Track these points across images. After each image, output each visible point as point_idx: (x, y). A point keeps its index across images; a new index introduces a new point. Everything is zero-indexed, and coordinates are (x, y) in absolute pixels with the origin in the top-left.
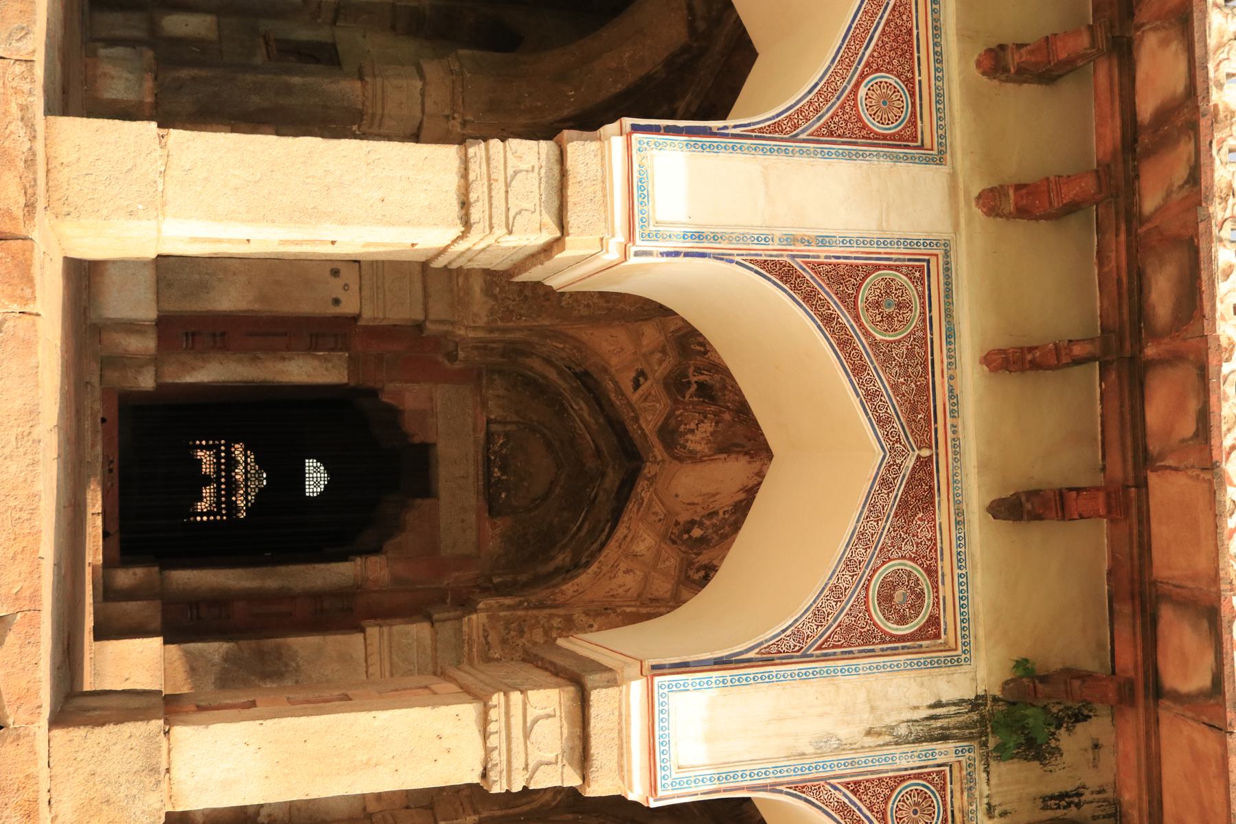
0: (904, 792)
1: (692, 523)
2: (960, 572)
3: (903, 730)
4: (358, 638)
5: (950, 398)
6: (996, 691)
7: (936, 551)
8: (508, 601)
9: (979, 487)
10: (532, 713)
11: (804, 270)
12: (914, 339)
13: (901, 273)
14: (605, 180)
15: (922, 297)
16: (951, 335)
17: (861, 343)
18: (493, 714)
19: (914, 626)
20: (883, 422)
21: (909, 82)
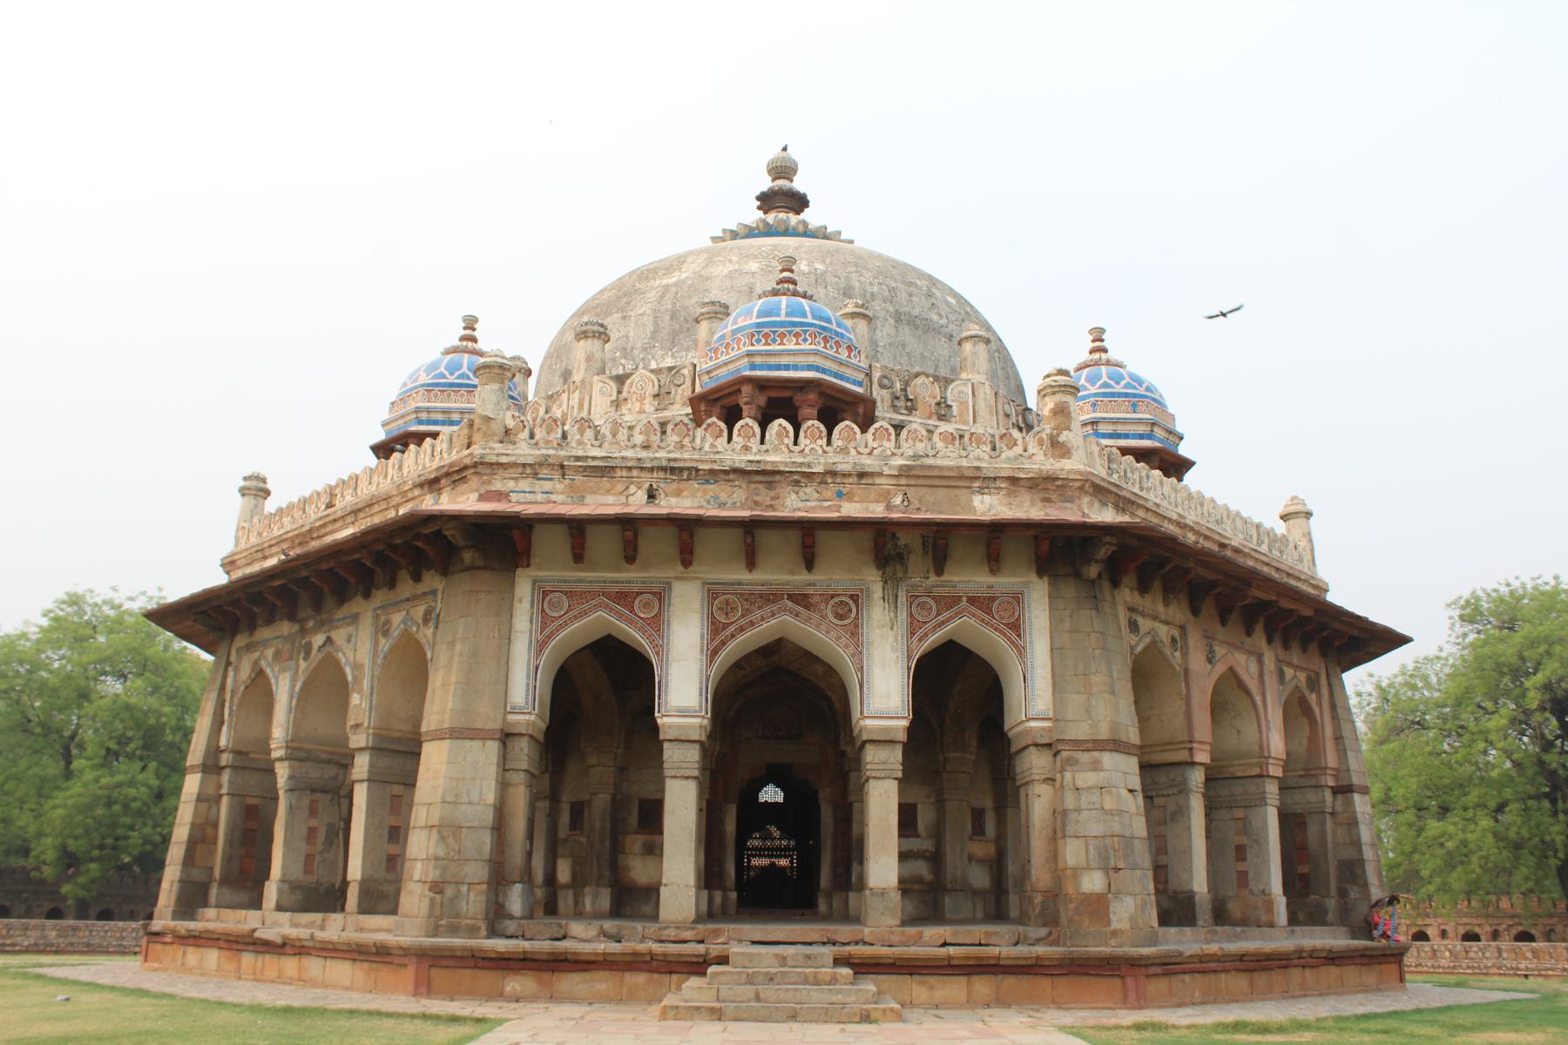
3: (892, 614)
6: (880, 573)
8: (842, 735)
14: (680, 727)
15: (724, 594)
16: (739, 584)
17: (742, 622)
20: (773, 614)
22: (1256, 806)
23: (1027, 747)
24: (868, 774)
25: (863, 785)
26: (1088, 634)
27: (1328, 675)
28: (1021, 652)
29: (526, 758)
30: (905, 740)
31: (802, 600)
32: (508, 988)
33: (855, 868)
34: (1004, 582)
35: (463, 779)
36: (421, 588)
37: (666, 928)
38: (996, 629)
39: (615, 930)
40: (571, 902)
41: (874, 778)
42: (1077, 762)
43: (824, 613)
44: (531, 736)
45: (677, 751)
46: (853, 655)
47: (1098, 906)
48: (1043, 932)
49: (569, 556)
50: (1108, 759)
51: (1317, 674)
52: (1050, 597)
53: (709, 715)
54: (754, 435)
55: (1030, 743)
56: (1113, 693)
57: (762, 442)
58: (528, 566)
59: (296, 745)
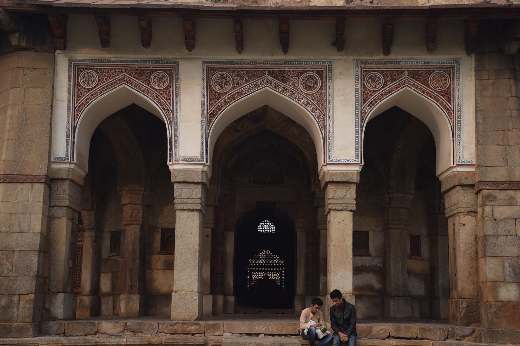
0: (368, 85)
2: (303, 64)
5: (251, 64)
7: (297, 70)
8: (313, 181)
9: (278, 56)
10: (336, 197)
11: (211, 110)
12: (232, 74)
13: (212, 77)
14: (186, 172)
15: (219, 71)
16: (231, 63)
17: (234, 92)
18: (334, 208)
19: (319, 79)
21: (153, 71)
23: (454, 187)
24: (330, 207)
25: (327, 215)
26: (507, 99)
28: (450, 113)
29: (67, 197)
30: (359, 181)
35: (15, 214)
37: (175, 324)
39: (135, 328)
40: (110, 306)
42: (495, 198)
43: (296, 85)
44: (72, 181)
45: (184, 191)
46: (319, 117)
48: (468, 330)
52: (476, 71)
53: (209, 163)
55: (457, 183)
58: (65, 48)
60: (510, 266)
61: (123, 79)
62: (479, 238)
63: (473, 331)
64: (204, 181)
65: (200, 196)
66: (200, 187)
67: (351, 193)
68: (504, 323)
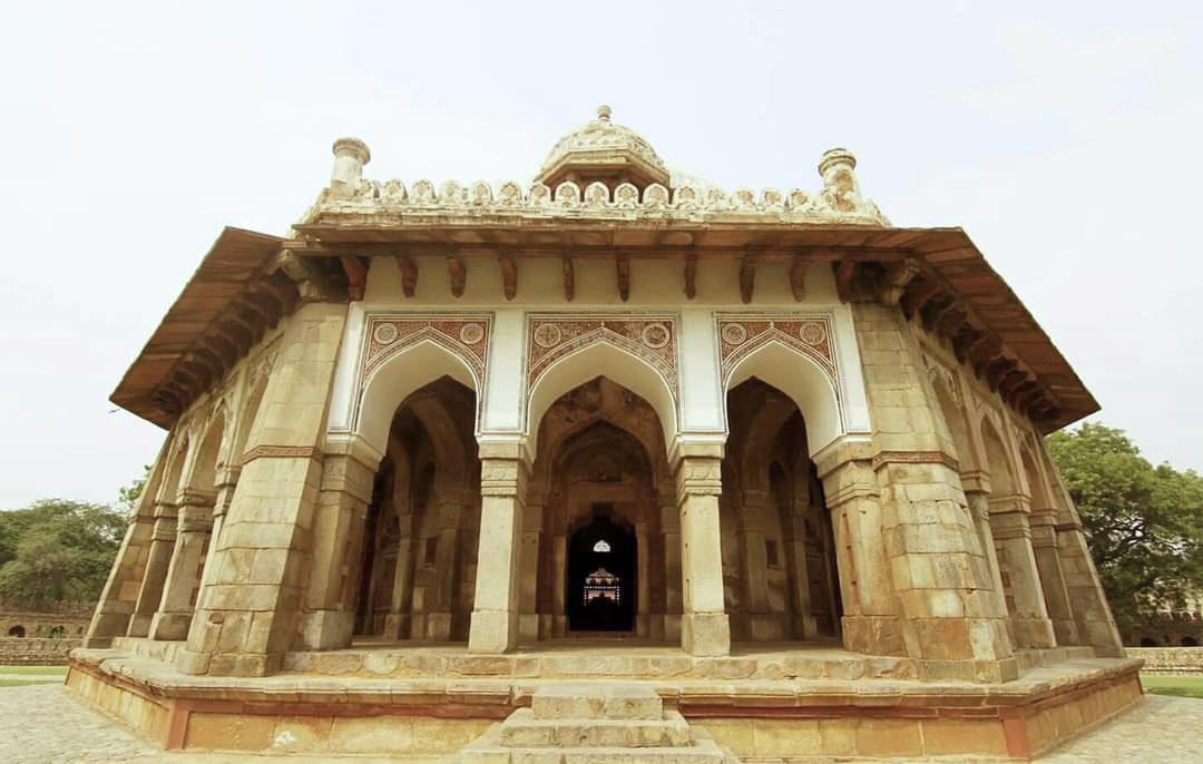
1: (627, 402)
4: (668, 536)
14: (497, 444)
17: (560, 347)
22: (1013, 538)
23: (846, 464)
24: (687, 490)
25: (681, 506)
27: (1038, 437)
29: (344, 478)
31: (619, 327)
32: (279, 739)
33: (670, 593)
34: (810, 308)
35: (267, 497)
36: (278, 332)
38: (805, 351)
41: (694, 494)
42: (906, 474)
44: (352, 458)
47: (954, 632)
48: (891, 661)
49: (401, 291)
50: (938, 471)
51: (1031, 434)
53: (528, 434)
54: (574, 194)
56: (929, 407)
57: (582, 199)
58: (361, 299)
59: (193, 492)
60: (941, 566)
61: (427, 333)
62: (889, 529)
63: (899, 664)
64: (522, 457)
65: (515, 476)
66: (516, 464)
67: (716, 471)
68: (947, 652)
